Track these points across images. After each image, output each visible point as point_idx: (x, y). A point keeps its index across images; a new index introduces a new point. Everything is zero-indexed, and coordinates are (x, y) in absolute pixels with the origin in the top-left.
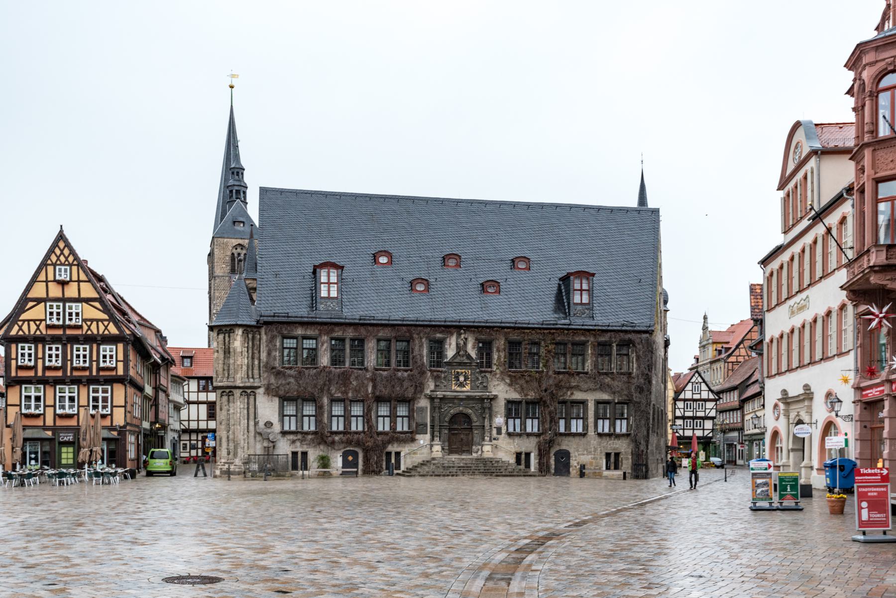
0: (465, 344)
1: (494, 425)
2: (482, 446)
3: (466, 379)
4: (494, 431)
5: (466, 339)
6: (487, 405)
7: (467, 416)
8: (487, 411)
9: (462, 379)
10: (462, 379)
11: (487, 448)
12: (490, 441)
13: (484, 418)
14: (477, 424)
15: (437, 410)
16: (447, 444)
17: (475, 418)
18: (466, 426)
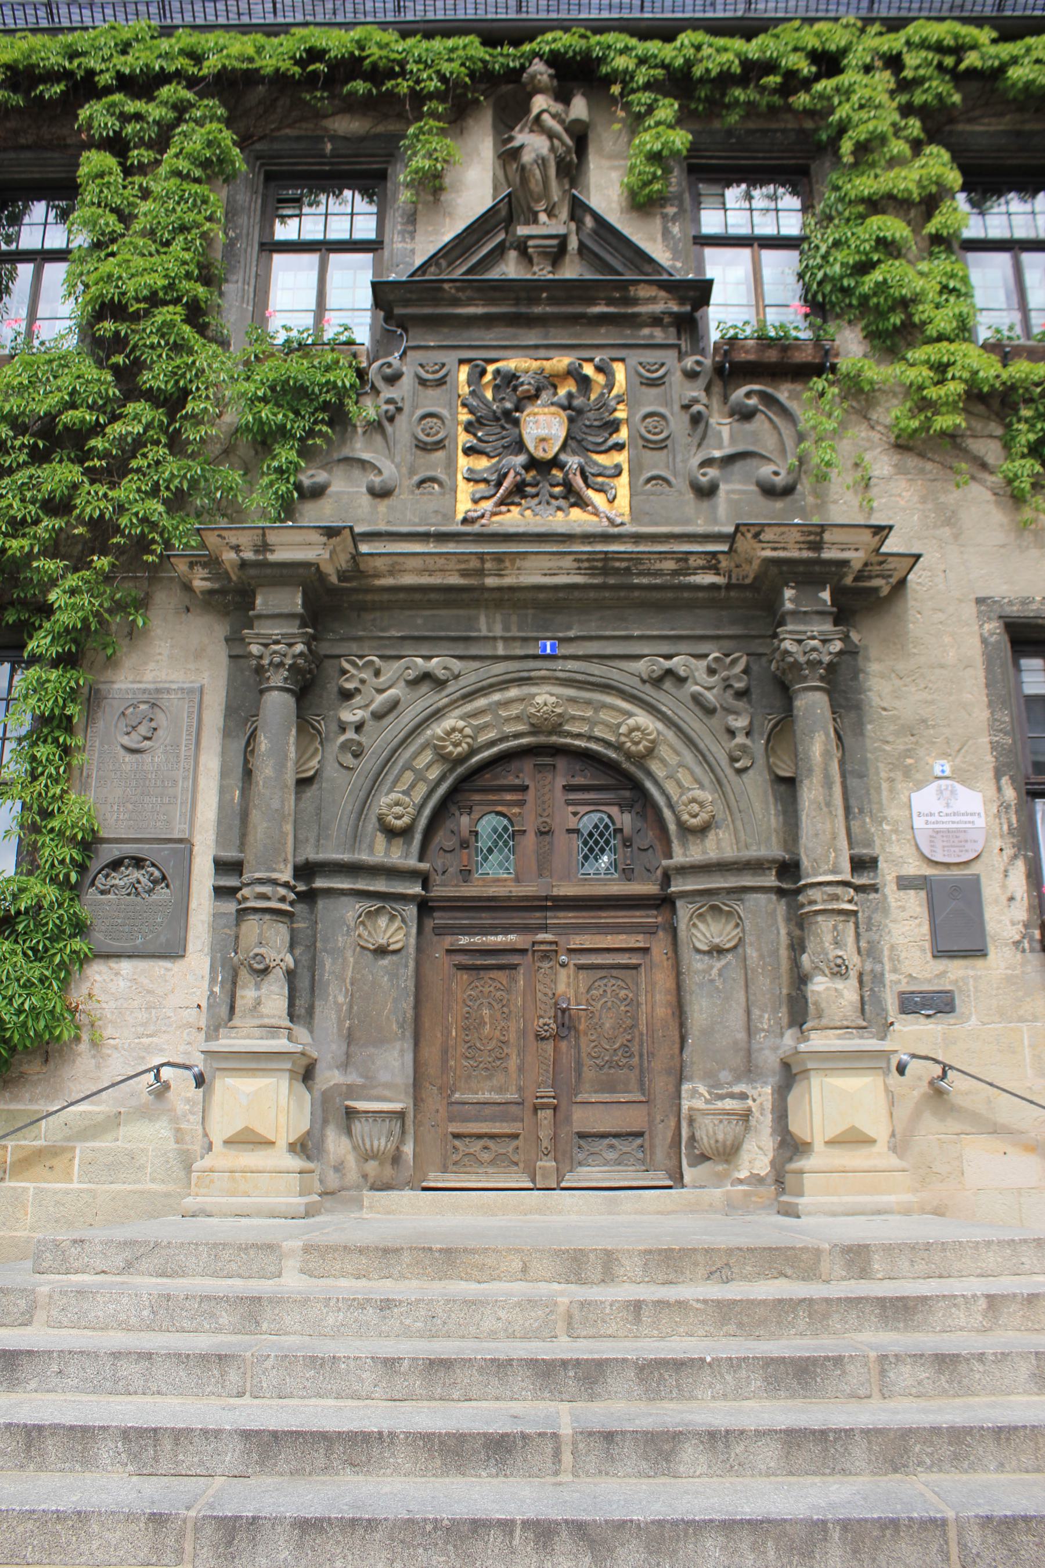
0: (571, 168)
1: (897, 860)
2: (790, 1075)
3: (589, 427)
4: (906, 923)
5: (580, 137)
6: (807, 635)
7: (618, 777)
8: (812, 703)
9: (544, 427)
10: (544, 427)
11: (835, 1100)
12: (870, 1015)
13: (787, 787)
14: (717, 846)
15: (278, 704)
16: (394, 1063)
17: (681, 783)
18: (600, 876)
